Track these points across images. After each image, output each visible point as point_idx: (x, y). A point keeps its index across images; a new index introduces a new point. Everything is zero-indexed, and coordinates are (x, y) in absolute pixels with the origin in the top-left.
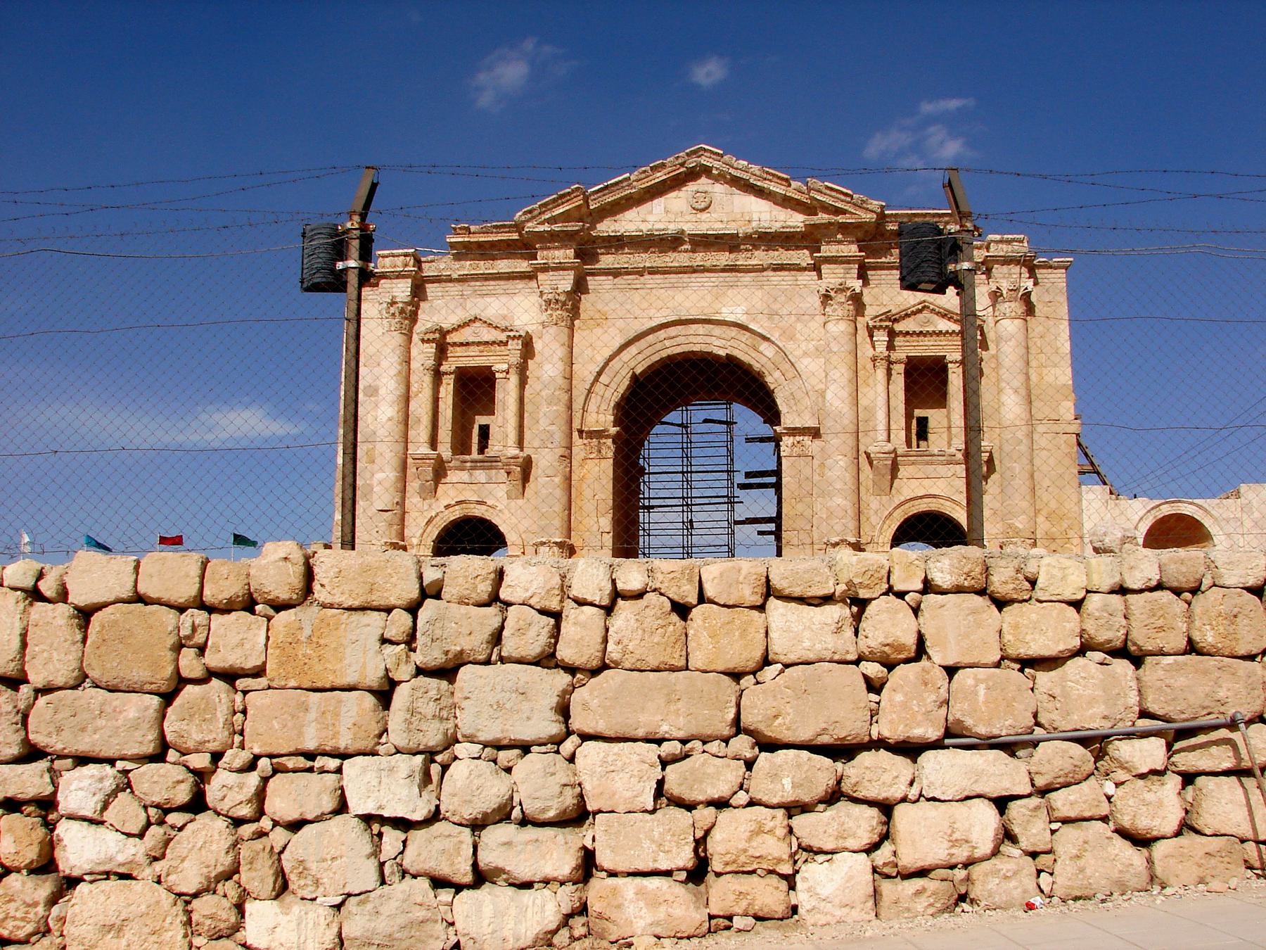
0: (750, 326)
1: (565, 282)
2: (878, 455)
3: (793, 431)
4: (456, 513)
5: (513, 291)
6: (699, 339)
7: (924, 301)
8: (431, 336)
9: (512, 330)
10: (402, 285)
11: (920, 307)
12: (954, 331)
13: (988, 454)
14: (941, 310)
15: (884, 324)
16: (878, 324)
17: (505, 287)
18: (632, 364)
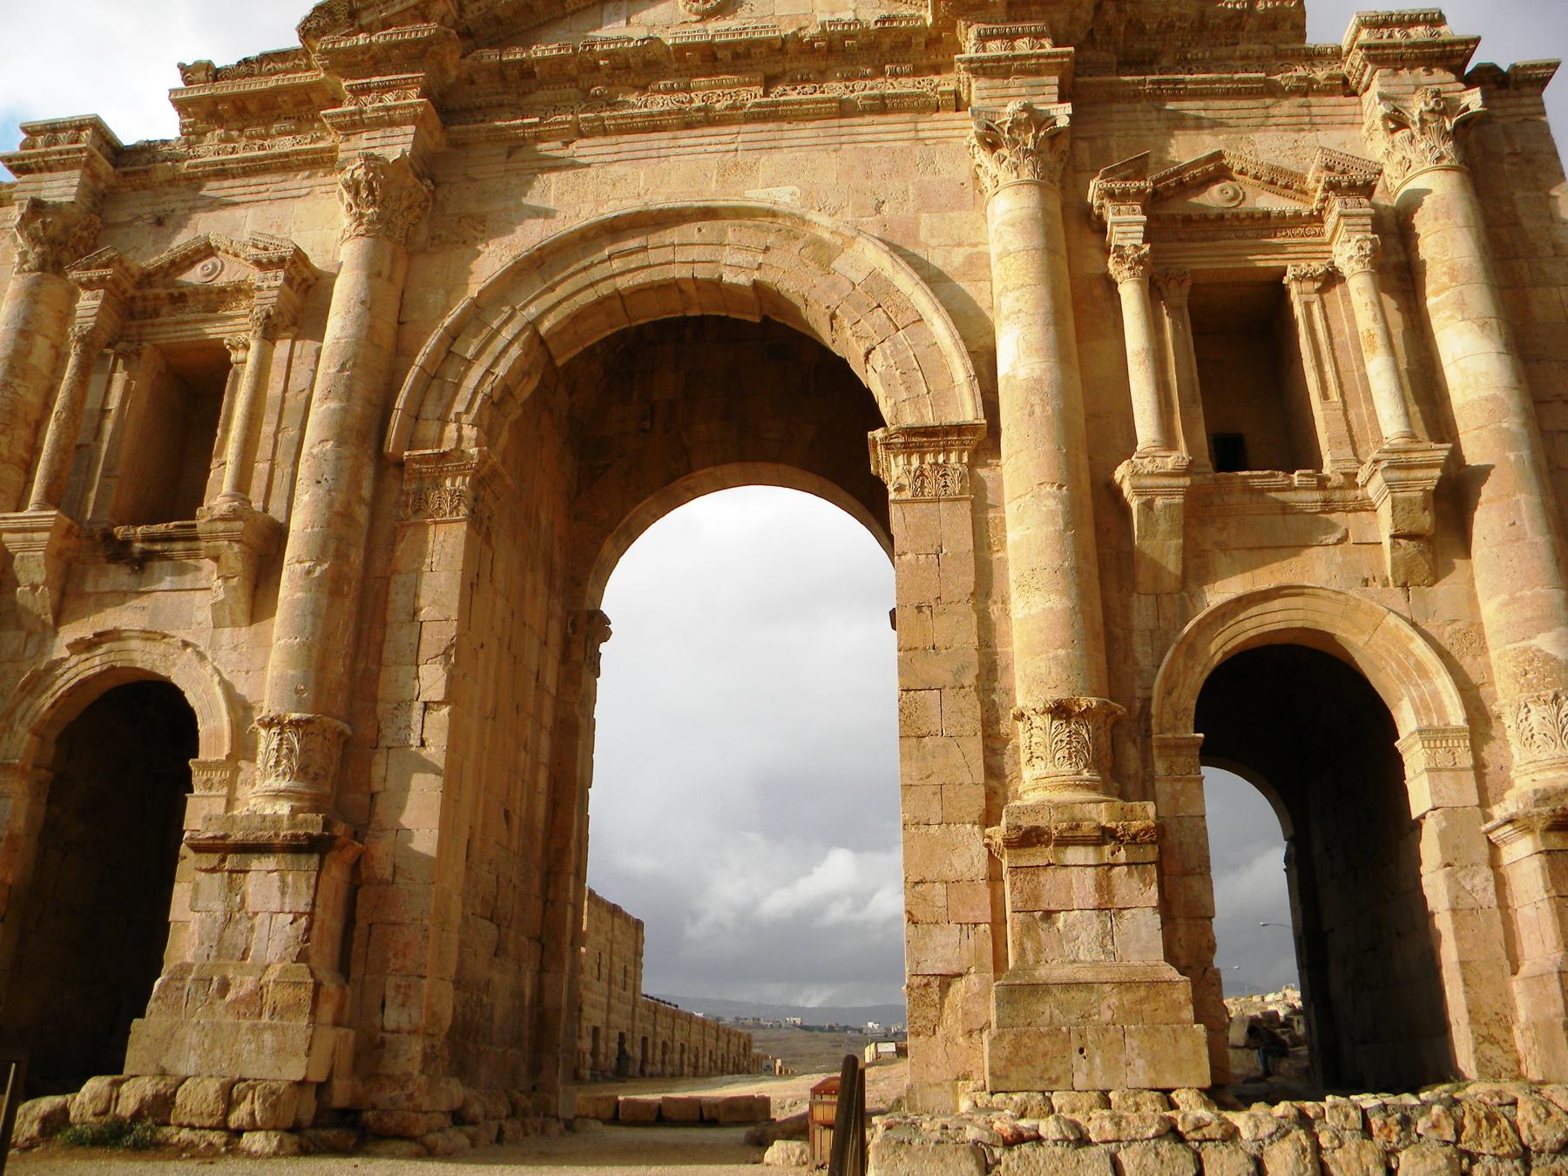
0: (808, 217)
1: (396, 145)
2: (1148, 482)
3: (922, 438)
4: (94, 664)
5: (295, 193)
6: (694, 253)
7: (1218, 156)
8: (95, 274)
9: (266, 249)
10: (61, 183)
11: (1211, 167)
12: (1297, 215)
13: (1437, 473)
14: (1263, 171)
15: (1133, 185)
16: (1117, 186)
17: (281, 186)
18: (533, 311)
